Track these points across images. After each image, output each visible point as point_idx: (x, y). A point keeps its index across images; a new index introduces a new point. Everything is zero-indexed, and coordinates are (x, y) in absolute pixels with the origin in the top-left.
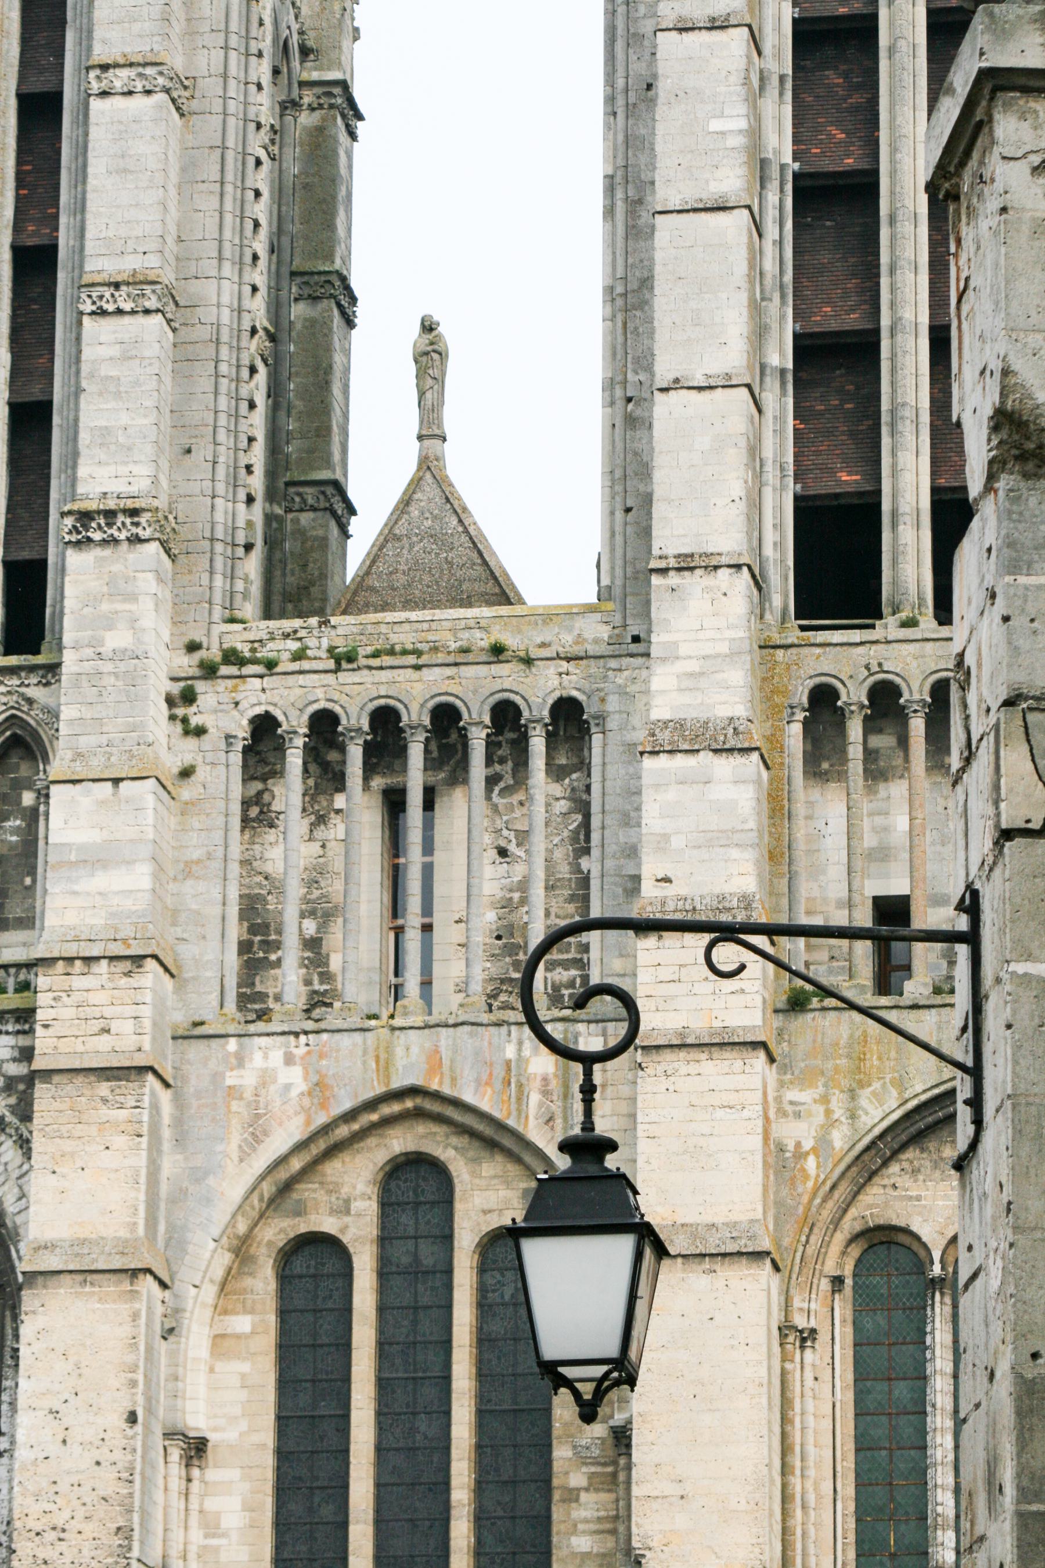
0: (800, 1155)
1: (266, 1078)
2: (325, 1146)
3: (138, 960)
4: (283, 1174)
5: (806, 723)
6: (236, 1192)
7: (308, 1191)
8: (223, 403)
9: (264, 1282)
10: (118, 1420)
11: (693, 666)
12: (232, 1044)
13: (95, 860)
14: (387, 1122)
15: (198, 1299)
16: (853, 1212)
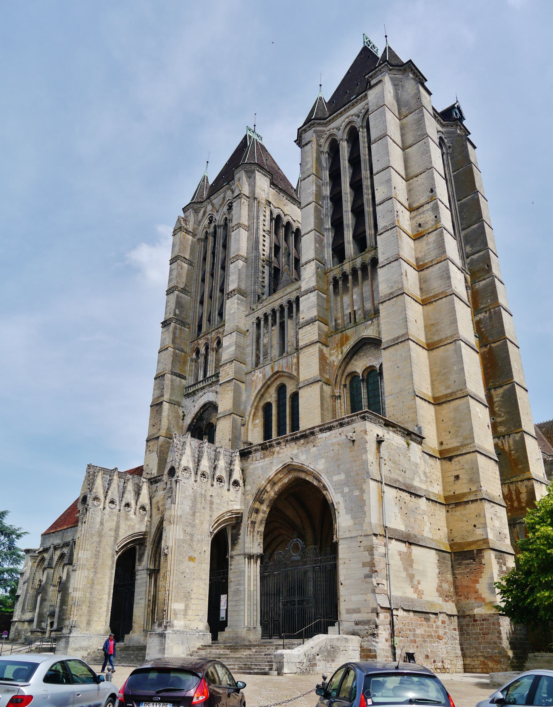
0: (334, 362)
1: (257, 376)
2: (266, 387)
3: (232, 361)
4: (261, 393)
5: (333, 285)
6: (253, 398)
7: (267, 395)
8: (253, 271)
9: (260, 413)
10: (228, 440)
11: (307, 280)
12: (253, 373)
13: (228, 347)
14: (276, 379)
15: (249, 418)
16: (346, 371)
